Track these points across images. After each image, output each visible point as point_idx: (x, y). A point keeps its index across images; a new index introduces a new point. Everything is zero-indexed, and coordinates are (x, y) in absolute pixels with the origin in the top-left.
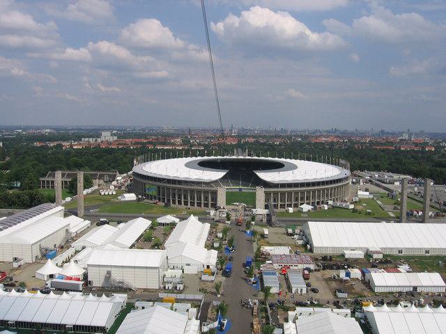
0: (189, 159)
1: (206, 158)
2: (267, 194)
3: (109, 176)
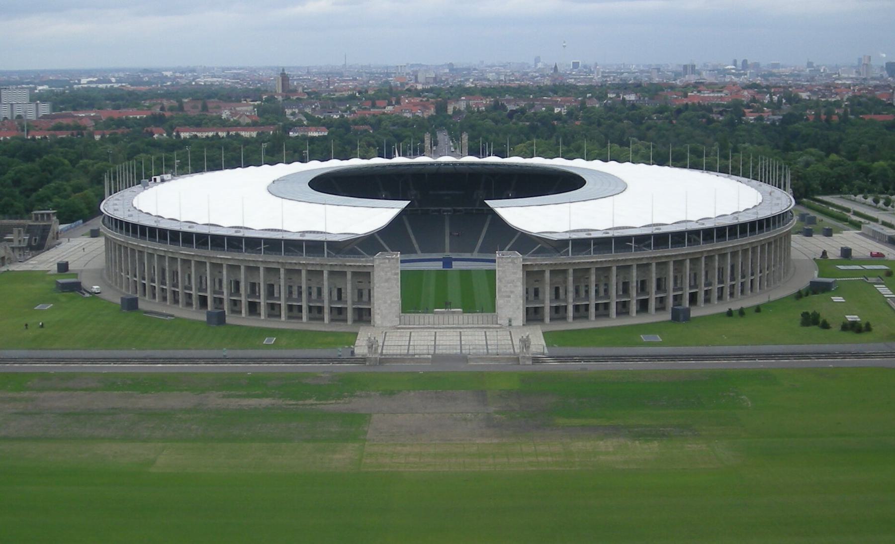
0: (282, 170)
1: (335, 164)
2: (531, 275)
3: (29, 230)
